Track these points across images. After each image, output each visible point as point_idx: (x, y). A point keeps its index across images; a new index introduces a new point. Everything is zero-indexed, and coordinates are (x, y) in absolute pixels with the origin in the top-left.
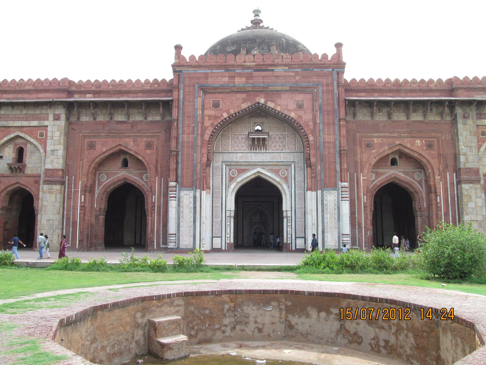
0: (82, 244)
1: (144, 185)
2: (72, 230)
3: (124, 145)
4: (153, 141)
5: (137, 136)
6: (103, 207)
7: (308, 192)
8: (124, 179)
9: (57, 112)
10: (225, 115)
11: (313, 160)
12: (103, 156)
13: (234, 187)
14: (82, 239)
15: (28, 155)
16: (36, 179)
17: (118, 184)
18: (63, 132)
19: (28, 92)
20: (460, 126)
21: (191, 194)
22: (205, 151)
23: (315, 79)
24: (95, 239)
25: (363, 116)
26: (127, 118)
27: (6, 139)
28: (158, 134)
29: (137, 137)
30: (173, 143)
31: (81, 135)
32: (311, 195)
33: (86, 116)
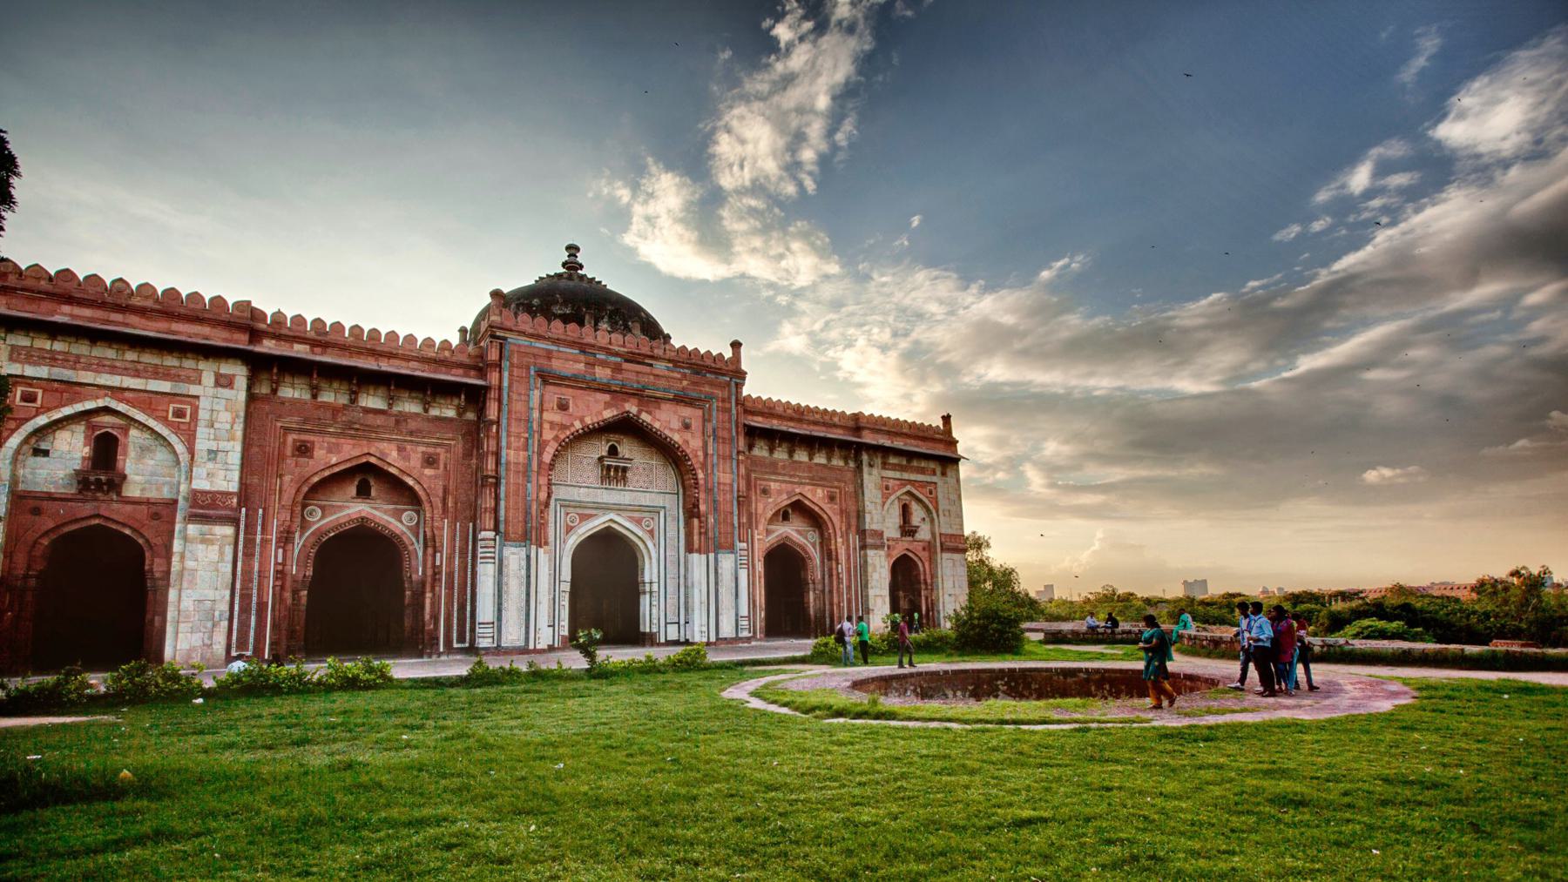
7: (696, 555)
9: (228, 368)
10: (578, 425)
11: (703, 508)
13: (573, 541)
15: (132, 453)
16: (154, 509)
18: (242, 414)
19: (142, 312)
20: (866, 476)
21: (523, 552)
22: (543, 481)
23: (707, 389)
25: (761, 451)
27: (68, 411)
30: (491, 464)
32: (697, 560)
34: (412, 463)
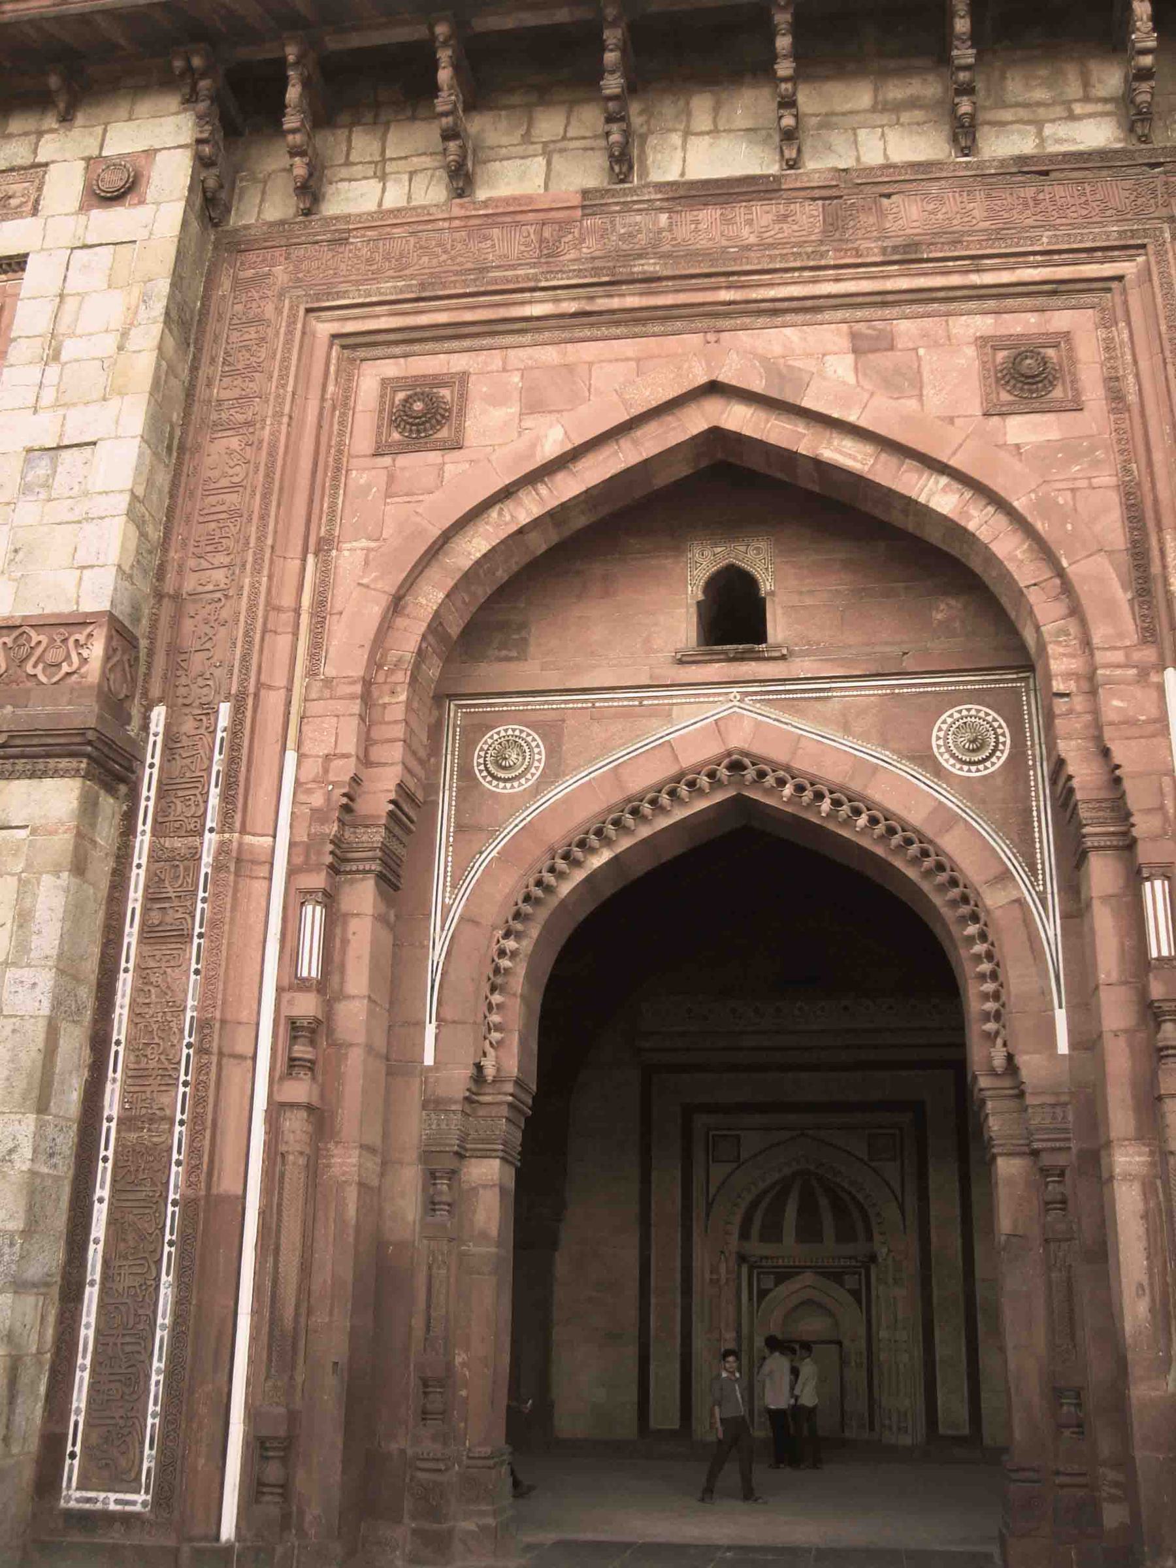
0: (285, 1489)
1: (951, 820)
2: (180, 1302)
3: (757, 385)
4: (1067, 335)
5: (883, 300)
6: (512, 1066)
8: (723, 773)
12: (536, 511)
14: (293, 1417)
17: (663, 822)
24: (425, 1415)
26: (789, 136)
28: (1108, 270)
29: (887, 312)
31: (324, 328)
33: (383, 178)
34: (935, 401)
